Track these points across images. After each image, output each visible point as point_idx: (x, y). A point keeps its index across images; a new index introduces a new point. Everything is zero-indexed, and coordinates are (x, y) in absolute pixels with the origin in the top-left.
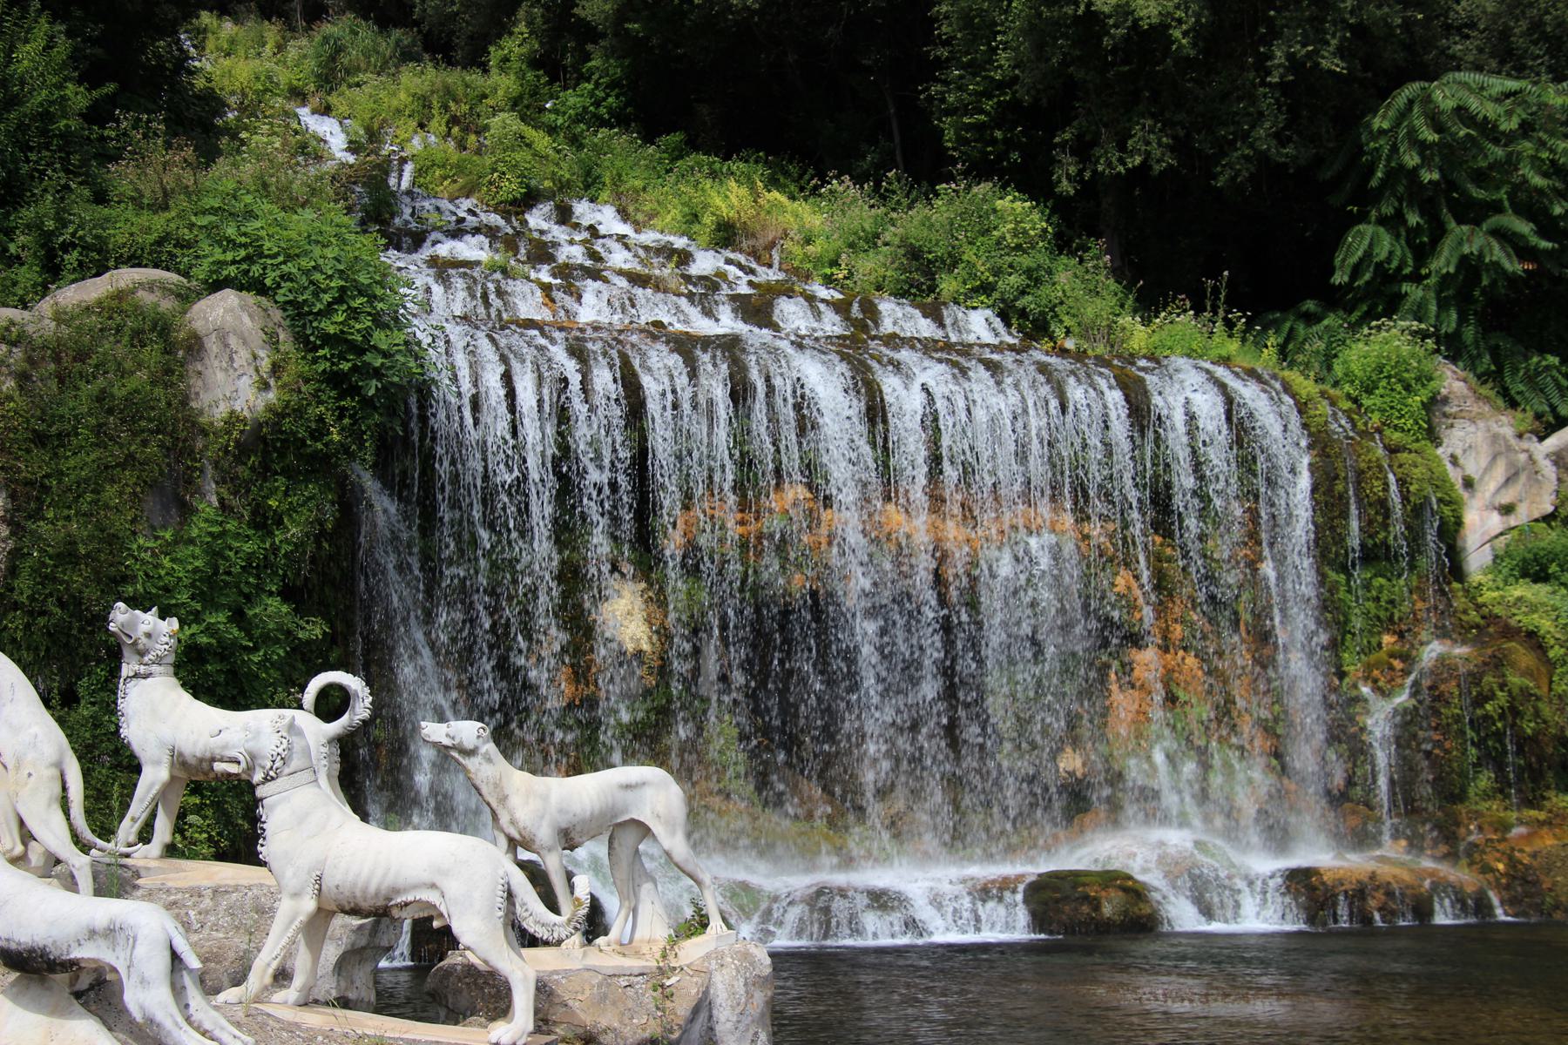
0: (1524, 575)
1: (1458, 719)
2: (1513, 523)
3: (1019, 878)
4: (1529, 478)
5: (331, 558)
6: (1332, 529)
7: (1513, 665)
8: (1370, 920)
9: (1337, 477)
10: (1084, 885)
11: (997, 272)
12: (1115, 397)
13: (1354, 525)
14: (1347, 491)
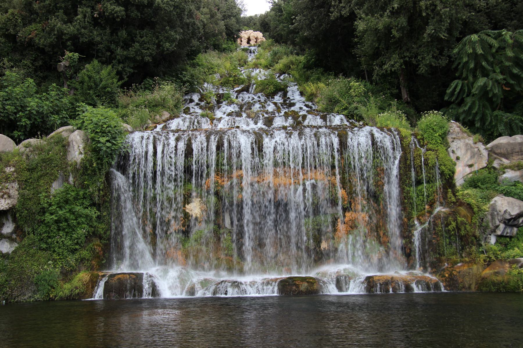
0: (471, 186)
1: (440, 231)
2: (473, 170)
3: (277, 279)
5: (103, 196)
6: (406, 175)
7: (459, 214)
8: (388, 291)
9: (408, 159)
10: (295, 281)
12: (336, 141)
13: (413, 174)
14: (411, 163)
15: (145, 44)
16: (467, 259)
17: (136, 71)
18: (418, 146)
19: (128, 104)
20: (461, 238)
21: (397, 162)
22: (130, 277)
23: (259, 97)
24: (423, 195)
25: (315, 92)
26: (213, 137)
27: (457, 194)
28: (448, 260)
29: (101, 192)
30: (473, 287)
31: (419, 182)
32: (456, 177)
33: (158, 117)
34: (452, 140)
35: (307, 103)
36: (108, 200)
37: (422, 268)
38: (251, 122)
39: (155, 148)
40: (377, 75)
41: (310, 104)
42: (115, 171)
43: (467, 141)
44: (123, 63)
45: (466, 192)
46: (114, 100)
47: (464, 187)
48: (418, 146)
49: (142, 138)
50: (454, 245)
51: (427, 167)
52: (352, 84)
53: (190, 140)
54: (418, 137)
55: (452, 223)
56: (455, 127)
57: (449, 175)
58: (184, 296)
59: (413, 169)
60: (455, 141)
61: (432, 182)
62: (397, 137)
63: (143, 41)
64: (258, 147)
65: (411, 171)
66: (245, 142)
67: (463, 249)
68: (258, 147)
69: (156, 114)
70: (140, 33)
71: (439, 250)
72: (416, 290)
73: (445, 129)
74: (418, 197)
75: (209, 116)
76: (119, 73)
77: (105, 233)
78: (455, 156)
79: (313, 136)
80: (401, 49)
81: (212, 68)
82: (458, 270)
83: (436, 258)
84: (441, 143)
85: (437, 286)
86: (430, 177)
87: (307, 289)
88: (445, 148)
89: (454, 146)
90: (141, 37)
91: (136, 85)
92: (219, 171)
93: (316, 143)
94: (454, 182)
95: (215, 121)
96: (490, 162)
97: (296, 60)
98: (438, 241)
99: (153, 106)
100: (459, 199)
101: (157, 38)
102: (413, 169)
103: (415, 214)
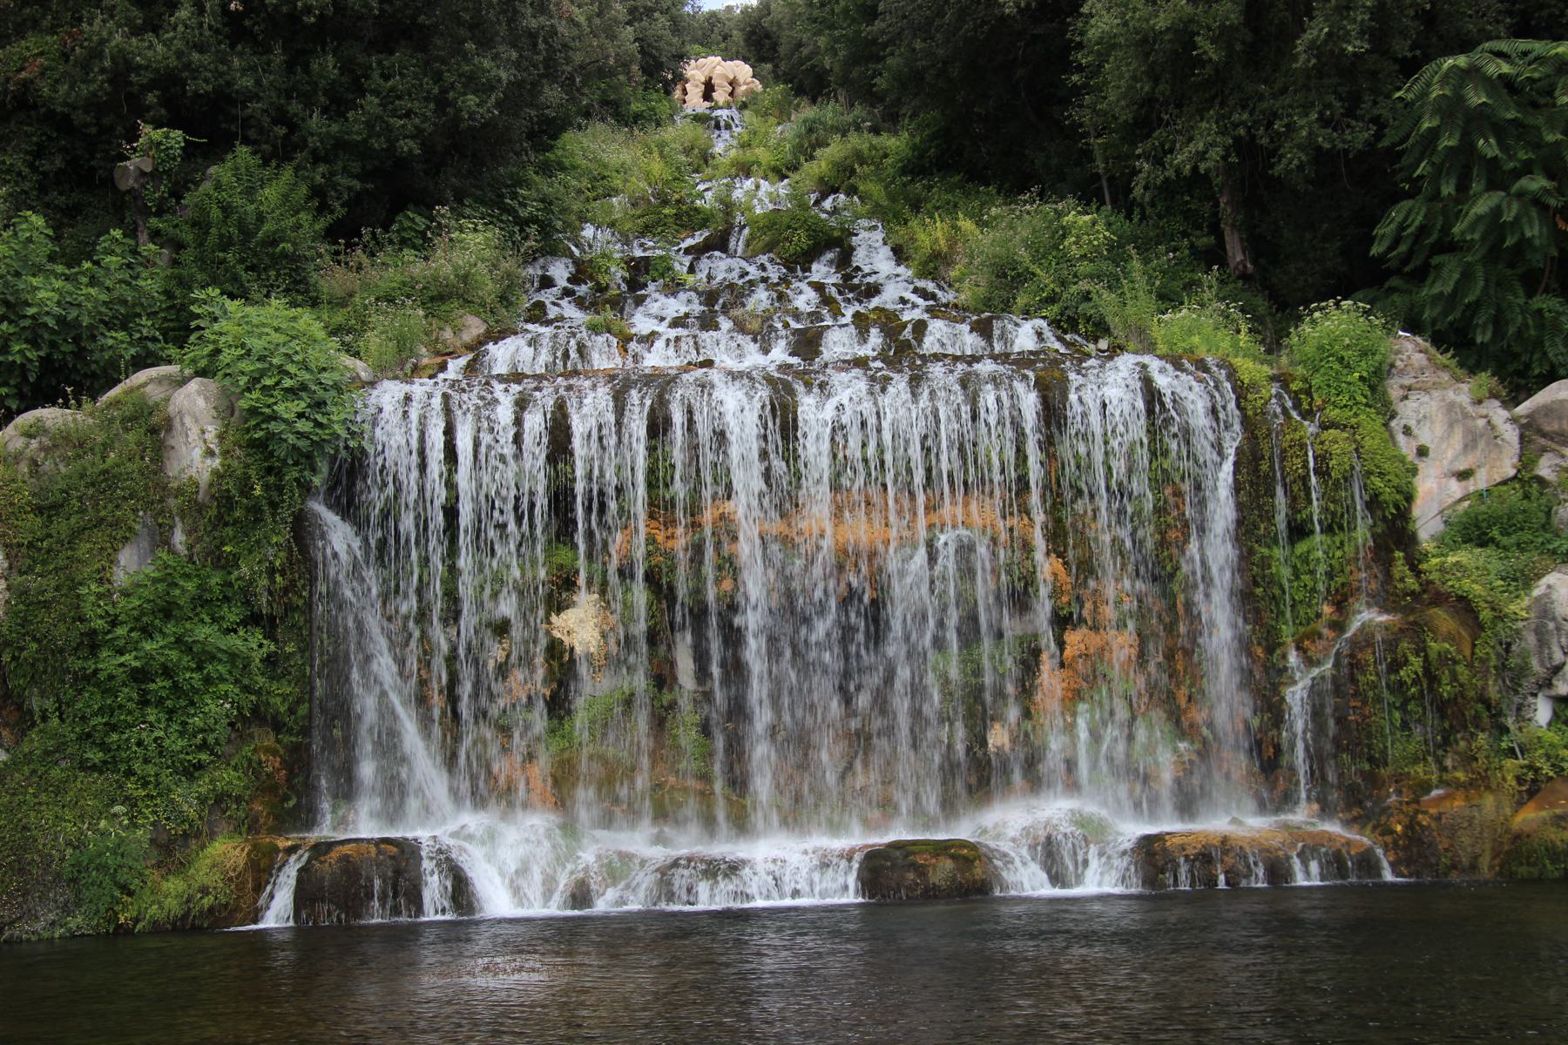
1: (1374, 686)
2: (1472, 489)
4: (1488, 444)
5: (286, 590)
6: (1259, 507)
9: (1263, 457)
10: (914, 853)
11: (1063, 284)
12: (1030, 402)
15: (399, 98)
16: (1461, 775)
17: (370, 186)
18: (1294, 414)
19: (351, 295)
20: (1442, 707)
21: (1228, 467)
22: (379, 852)
23: (763, 268)
24: (1312, 572)
25: (945, 250)
26: (634, 394)
27: (1424, 566)
28: (1398, 778)
29: (278, 579)
30: (1485, 862)
31: (1298, 531)
32: (1417, 511)
33: (448, 334)
34: (1401, 393)
35: (921, 284)
36: (300, 603)
37: (1316, 806)
38: (752, 348)
39: (449, 432)
40: (1146, 188)
41: (930, 286)
42: (318, 507)
43: (1451, 395)
44: (326, 160)
45: (1451, 559)
46: (304, 281)
47: (1446, 543)
48: (1294, 414)
49: (408, 399)
50: (1418, 731)
51: (1326, 483)
52: (1070, 218)
53: (561, 406)
54: (1294, 387)
55: (1412, 659)
56: (1410, 350)
57: (1397, 507)
58: (555, 909)
59: (1279, 491)
60: (1413, 396)
61: (1341, 528)
62: (1228, 385)
63: (392, 89)
64: (783, 421)
65: (1273, 496)
66: (739, 412)
67: (1446, 742)
68: (783, 421)
69: (441, 324)
70: (380, 63)
71: (1370, 747)
72: (1307, 876)
73: (1378, 357)
74: (1297, 578)
75: (615, 328)
76: (317, 192)
77: (292, 711)
78: (1414, 445)
79: (957, 387)
80: (1222, 104)
81: (604, 178)
82: (1433, 811)
83: (1361, 772)
84: (1366, 405)
85: (1367, 863)
86: (1334, 514)
87: (954, 878)
88: (1380, 420)
89: (1408, 411)
90: (386, 78)
91: (373, 233)
92: (660, 508)
93: (965, 410)
94: (1410, 527)
95: (633, 346)
96: (1526, 461)
97: (873, 147)
98: (1365, 717)
99: (432, 299)
100: (1432, 582)
101: (438, 78)
102: (1279, 491)
103: (1287, 631)
